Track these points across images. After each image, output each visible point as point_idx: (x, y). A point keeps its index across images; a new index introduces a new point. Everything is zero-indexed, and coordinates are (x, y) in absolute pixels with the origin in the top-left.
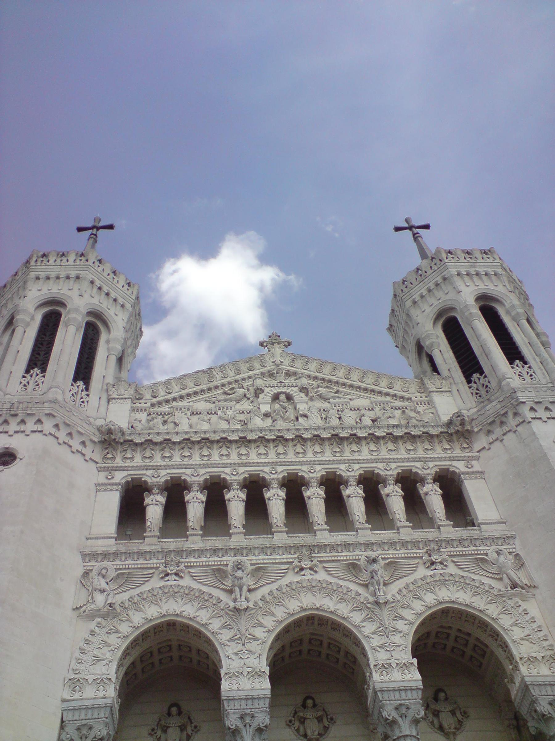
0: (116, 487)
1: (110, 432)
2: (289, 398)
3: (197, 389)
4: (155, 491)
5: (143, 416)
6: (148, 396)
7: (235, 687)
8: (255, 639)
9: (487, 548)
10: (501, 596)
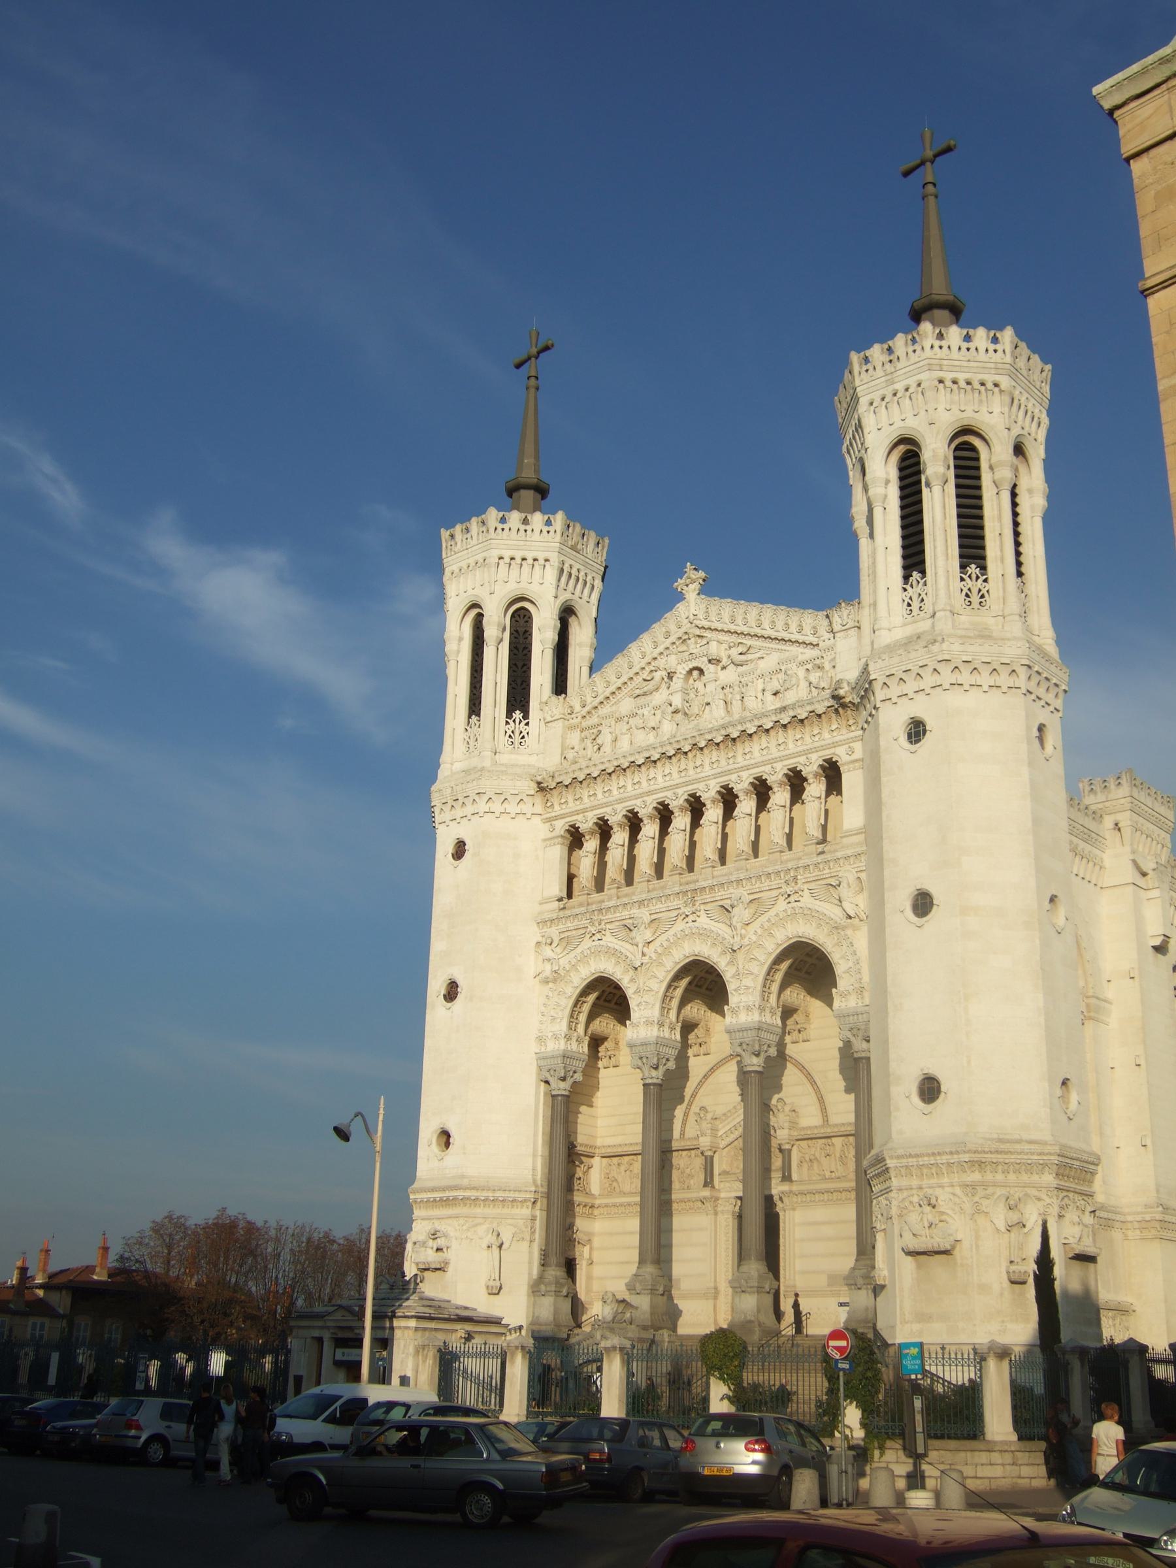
0: (556, 841)
1: (539, 783)
2: (701, 672)
3: (619, 683)
4: (587, 837)
5: (574, 738)
6: (577, 708)
7: (635, 1036)
8: (651, 990)
9: (839, 869)
10: (836, 928)
